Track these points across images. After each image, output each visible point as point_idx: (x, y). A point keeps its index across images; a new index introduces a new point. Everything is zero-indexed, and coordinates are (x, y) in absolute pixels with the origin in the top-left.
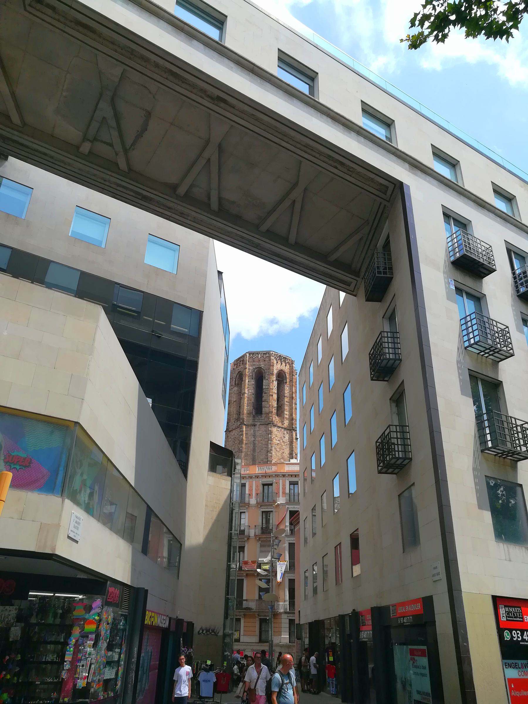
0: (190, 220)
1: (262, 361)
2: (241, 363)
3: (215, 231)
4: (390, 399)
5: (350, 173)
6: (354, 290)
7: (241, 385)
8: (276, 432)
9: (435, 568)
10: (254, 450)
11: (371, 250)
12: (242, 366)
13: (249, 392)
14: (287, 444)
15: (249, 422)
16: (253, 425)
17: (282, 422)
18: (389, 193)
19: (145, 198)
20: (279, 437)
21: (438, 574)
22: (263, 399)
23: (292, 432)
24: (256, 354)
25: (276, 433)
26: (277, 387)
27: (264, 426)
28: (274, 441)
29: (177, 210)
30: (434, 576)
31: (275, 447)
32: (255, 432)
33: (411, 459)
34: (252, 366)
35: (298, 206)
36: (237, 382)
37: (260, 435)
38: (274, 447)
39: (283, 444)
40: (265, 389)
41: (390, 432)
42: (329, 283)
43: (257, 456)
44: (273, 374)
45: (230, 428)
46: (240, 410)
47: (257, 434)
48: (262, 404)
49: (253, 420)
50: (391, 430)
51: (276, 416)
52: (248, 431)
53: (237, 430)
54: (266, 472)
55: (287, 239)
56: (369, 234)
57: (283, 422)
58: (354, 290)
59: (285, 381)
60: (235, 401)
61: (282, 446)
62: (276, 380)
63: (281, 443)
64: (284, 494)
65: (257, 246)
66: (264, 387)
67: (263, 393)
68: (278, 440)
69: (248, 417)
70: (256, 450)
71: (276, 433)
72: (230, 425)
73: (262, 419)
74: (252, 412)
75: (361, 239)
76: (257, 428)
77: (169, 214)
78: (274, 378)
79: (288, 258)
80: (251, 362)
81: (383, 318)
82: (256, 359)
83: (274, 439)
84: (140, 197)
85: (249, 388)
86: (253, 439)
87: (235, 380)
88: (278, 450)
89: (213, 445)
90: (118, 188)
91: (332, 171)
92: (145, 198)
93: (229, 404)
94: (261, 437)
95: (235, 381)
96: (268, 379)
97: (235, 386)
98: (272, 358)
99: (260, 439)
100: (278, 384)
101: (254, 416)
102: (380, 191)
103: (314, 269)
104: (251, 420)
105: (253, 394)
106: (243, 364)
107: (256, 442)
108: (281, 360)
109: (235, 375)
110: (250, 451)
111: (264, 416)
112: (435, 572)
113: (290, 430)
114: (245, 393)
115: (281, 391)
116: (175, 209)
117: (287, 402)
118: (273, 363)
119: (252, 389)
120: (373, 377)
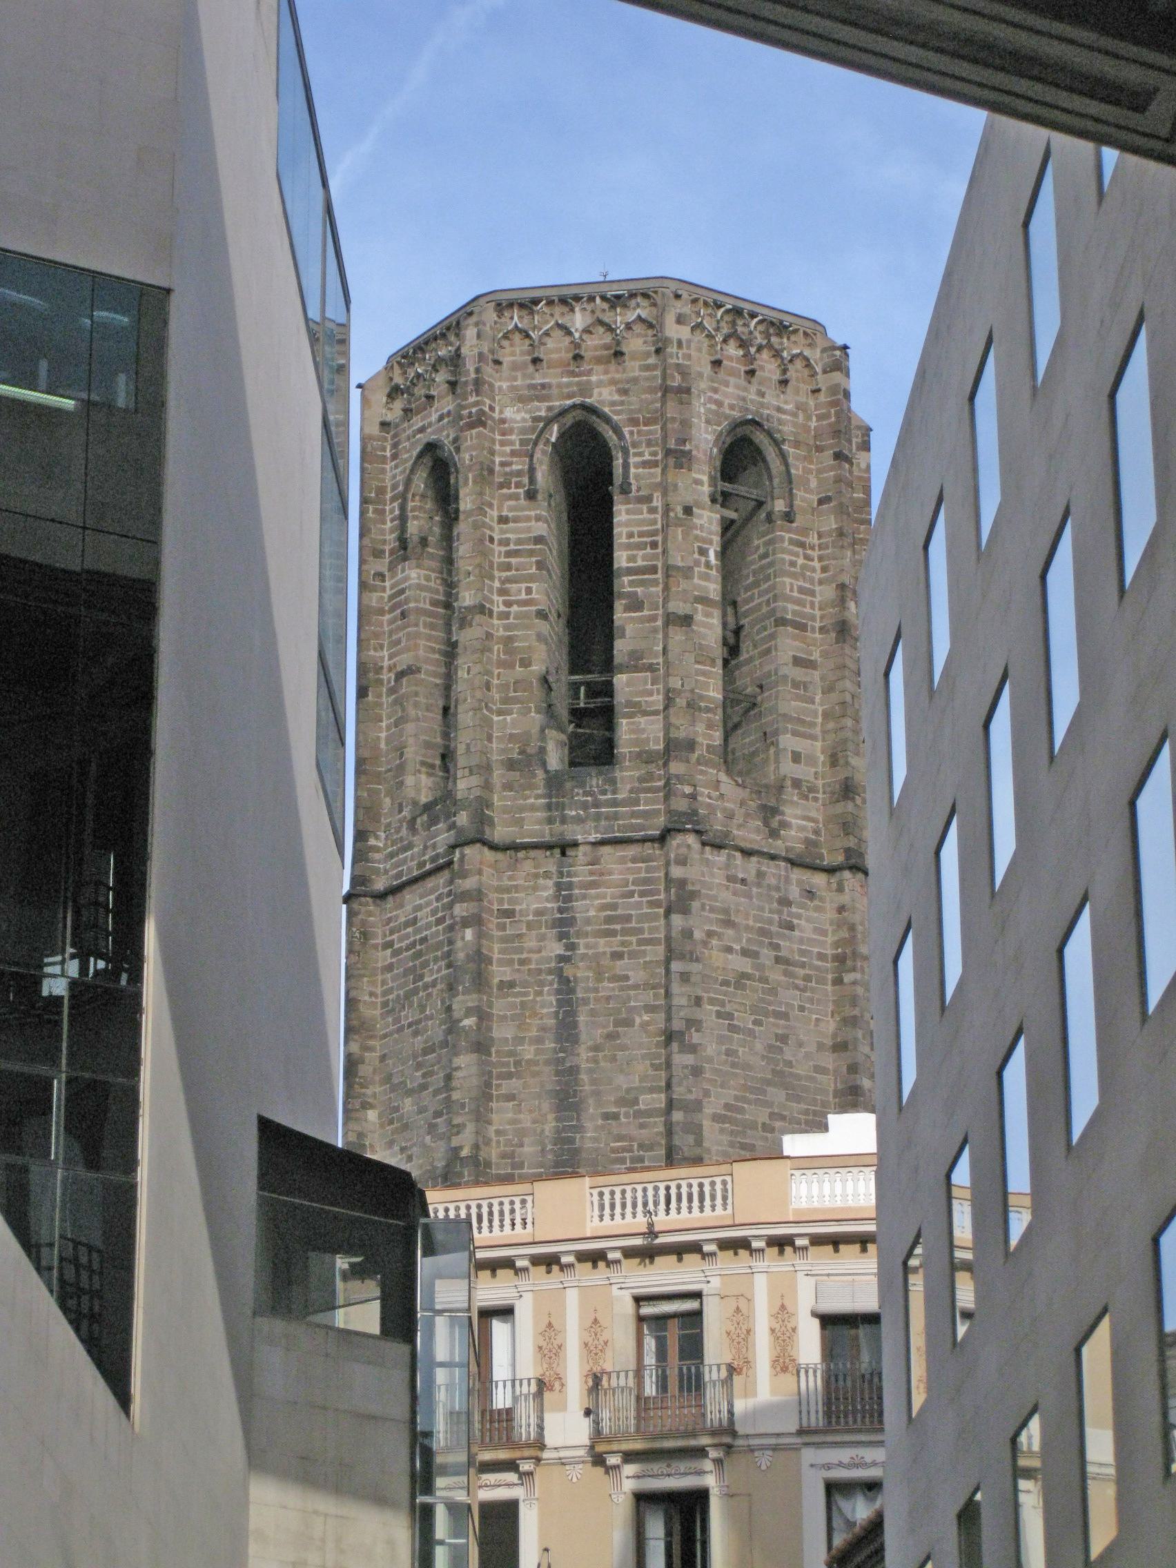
1: (599, 360)
2: (441, 377)
8: (725, 895)
10: (567, 1030)
13: (508, 604)
14: (807, 978)
15: (519, 822)
16: (549, 847)
17: (769, 812)
20: (747, 928)
22: (621, 647)
23: (840, 889)
25: (726, 897)
26: (723, 553)
27: (632, 851)
28: (716, 957)
31: (722, 1004)
32: (569, 899)
34: (521, 399)
37: (609, 920)
38: (712, 1001)
39: (776, 975)
40: (630, 571)
42: (1007, 99)
43: (590, 1071)
45: (377, 871)
47: (588, 909)
49: (549, 807)
51: (723, 777)
52: (516, 888)
53: (430, 883)
54: (651, 1225)
57: (774, 811)
59: (780, 506)
61: (773, 991)
63: (760, 967)
64: (784, 1369)
66: (621, 559)
67: (619, 605)
68: (745, 953)
69: (508, 787)
70: (582, 1026)
71: (726, 897)
72: (377, 850)
73: (614, 803)
74: (542, 750)
76: (580, 870)
80: (515, 367)
82: (550, 343)
83: (714, 942)
85: (508, 567)
87: (403, 508)
88: (745, 1020)
93: (362, 692)
94: (613, 933)
95: (403, 518)
96: (649, 499)
97: (405, 559)
98: (673, 331)
101: (554, 783)
104: (533, 808)
105: (542, 615)
106: (453, 385)
107: (581, 972)
108: (743, 344)
109: (393, 474)
110: (539, 1040)
111: (627, 774)
113: (831, 871)
114: (482, 609)
115: (747, 589)
117: (797, 661)
119: (531, 578)
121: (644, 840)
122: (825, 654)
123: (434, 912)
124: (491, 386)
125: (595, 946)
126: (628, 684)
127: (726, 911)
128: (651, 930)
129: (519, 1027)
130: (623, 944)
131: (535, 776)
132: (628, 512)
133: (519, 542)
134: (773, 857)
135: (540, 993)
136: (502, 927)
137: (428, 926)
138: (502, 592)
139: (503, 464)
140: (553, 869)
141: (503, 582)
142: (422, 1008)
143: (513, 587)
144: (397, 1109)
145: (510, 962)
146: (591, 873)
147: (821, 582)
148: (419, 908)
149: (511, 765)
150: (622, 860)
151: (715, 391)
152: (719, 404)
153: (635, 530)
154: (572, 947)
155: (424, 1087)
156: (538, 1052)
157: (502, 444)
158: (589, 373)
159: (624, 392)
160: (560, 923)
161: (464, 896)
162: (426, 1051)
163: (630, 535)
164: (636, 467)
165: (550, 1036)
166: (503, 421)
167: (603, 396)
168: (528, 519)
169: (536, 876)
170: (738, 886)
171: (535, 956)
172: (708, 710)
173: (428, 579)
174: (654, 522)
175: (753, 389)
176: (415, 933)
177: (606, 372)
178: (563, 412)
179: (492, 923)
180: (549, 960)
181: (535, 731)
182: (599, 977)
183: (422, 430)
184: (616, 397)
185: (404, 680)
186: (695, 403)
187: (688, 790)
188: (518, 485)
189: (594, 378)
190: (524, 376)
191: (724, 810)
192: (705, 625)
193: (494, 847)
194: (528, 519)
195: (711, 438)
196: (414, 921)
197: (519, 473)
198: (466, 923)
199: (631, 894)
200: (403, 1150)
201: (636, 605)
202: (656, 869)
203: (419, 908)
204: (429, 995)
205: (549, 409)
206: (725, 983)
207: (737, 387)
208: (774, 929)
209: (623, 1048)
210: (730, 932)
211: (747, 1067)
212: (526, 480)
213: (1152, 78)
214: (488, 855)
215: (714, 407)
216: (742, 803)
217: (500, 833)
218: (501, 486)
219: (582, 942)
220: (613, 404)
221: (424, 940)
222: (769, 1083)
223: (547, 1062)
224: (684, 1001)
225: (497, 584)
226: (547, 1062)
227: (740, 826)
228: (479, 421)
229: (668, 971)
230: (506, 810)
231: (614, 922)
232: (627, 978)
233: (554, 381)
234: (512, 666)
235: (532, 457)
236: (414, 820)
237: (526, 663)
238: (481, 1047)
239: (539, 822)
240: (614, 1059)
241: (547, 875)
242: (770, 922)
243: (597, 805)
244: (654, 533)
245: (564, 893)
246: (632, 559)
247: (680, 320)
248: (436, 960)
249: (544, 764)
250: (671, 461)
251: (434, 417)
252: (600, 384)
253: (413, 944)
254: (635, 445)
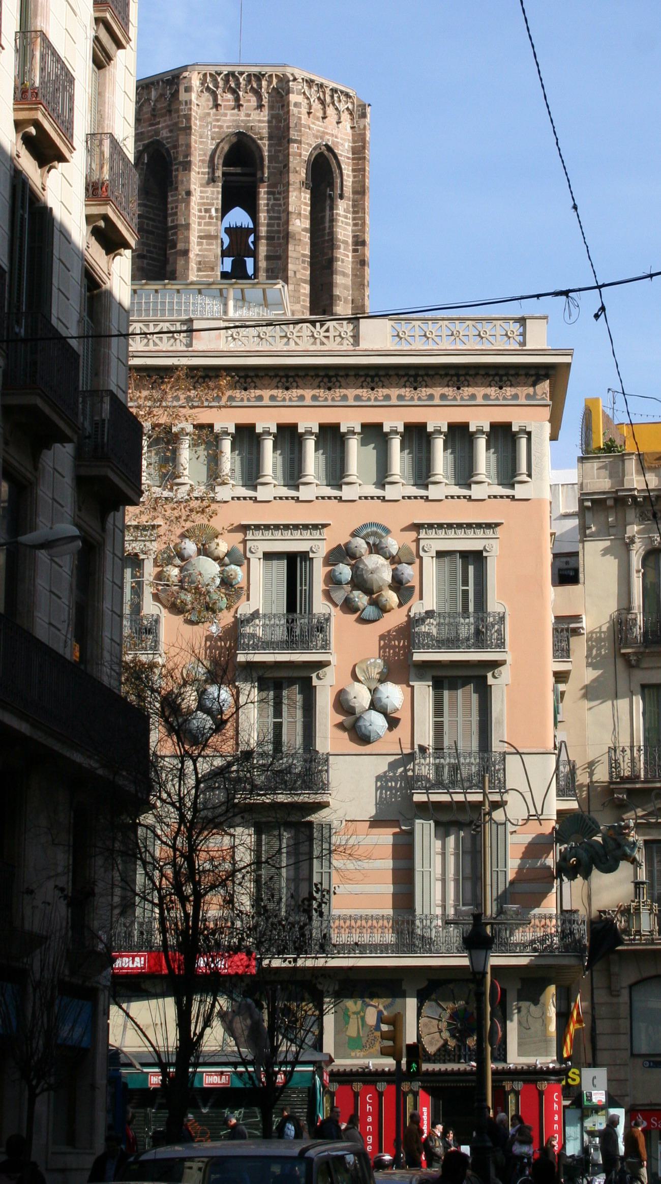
151: (218, 120)
158: (158, 123)
175: (242, 113)
189: (160, 126)
205: (144, 145)
207: (232, 115)
215: (217, 130)
220: (167, 138)
252: (163, 128)
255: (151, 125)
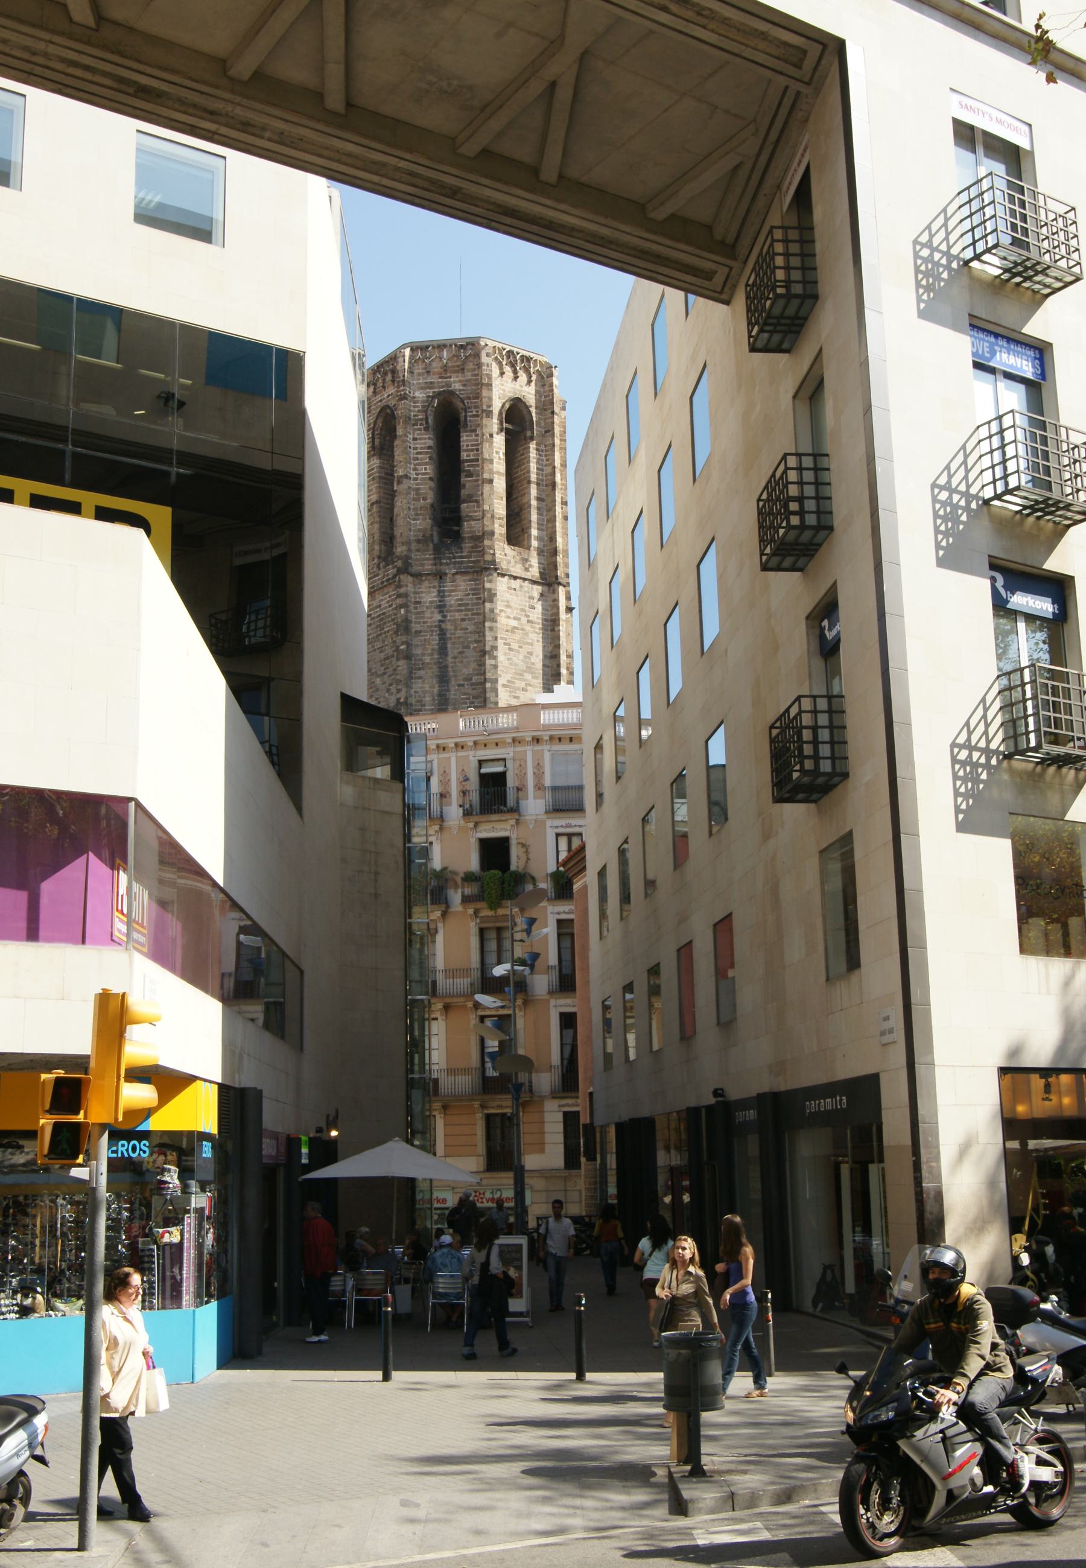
0: (270, 140)
1: (455, 372)
2: (389, 377)
3: (338, 161)
4: (807, 618)
5: (704, 21)
6: (723, 288)
7: (393, 451)
9: (887, 1019)
10: (443, 650)
11: (765, 195)
12: (391, 390)
15: (423, 565)
18: (809, 64)
19: (143, 92)
20: (516, 608)
21: (891, 1031)
22: (464, 493)
24: (434, 347)
27: (468, 577)
29: (232, 117)
30: (883, 1034)
31: (506, 639)
32: (443, 596)
33: (846, 775)
34: (422, 388)
35: (564, 94)
36: (377, 442)
37: (459, 605)
39: (528, 628)
41: (801, 712)
43: (452, 667)
44: (489, 414)
46: (392, 529)
47: (451, 601)
48: (457, 510)
49: (435, 559)
50: (803, 709)
51: (506, 546)
52: (422, 592)
53: (386, 590)
55: (536, 171)
56: (759, 155)
57: (527, 560)
58: (723, 288)
59: (529, 434)
60: (377, 502)
61: (526, 634)
62: (501, 430)
64: (539, 789)
65: (454, 193)
66: (464, 455)
67: (463, 475)
68: (515, 618)
69: (418, 550)
70: (449, 650)
73: (462, 557)
74: (432, 535)
75: (737, 168)
76: (448, 585)
77: (212, 127)
78: (493, 424)
79: (541, 218)
80: (419, 374)
81: (794, 397)
82: (434, 365)
83: (503, 614)
84: (131, 91)
85: (417, 459)
86: (438, 617)
88: (515, 646)
89: (349, 703)
90: (71, 70)
91: (656, 18)
92: (143, 92)
94: (461, 611)
96: (475, 431)
97: (374, 455)
98: (484, 359)
99: (458, 616)
100: (508, 443)
101: (437, 550)
102: (786, 61)
103: (611, 242)
104: (428, 559)
106: (393, 381)
107: (448, 626)
111: (467, 545)
112: (886, 1025)
114: (406, 477)
116: (227, 114)
118: (490, 377)
119: (426, 464)
120: (768, 561)
121: (474, 572)
122: (547, 495)
123: (388, 602)
124: (409, 383)
125: (454, 616)
126: (467, 507)
127: (508, 602)
128: (477, 609)
129: (423, 649)
130: (466, 615)
131: (428, 546)
132: (467, 436)
133: (421, 448)
134: (525, 579)
135: (432, 635)
136: (416, 608)
137: (385, 608)
138: (415, 469)
139: (414, 416)
140: (437, 584)
141: (415, 465)
142: (383, 641)
143: (419, 467)
144: (373, 683)
145: (419, 623)
146: (452, 586)
147: (546, 466)
148: (382, 600)
149: (419, 541)
150: (465, 581)
151: (502, 385)
152: (504, 390)
153: (470, 443)
154: (444, 616)
155: (384, 674)
156: (431, 659)
157: (414, 407)
158: (450, 377)
159: (464, 385)
160: (439, 607)
161: (399, 596)
162: (385, 659)
163: (467, 446)
164: (470, 416)
165: (436, 652)
166: (414, 397)
167: (457, 386)
168: (425, 439)
169: (430, 587)
170: (513, 591)
171: (429, 620)
172: (500, 519)
173: (383, 464)
174: (477, 440)
176: (380, 610)
177: (457, 377)
178: (439, 393)
179: (412, 606)
180: (435, 622)
181: (429, 527)
182: (456, 629)
183: (381, 401)
184: (461, 388)
185: (375, 506)
186: (494, 390)
187: (492, 552)
188: (421, 425)
190: (424, 379)
191: (506, 560)
192: (499, 483)
193: (412, 575)
194: (425, 439)
195: (500, 405)
196: (380, 606)
197: (421, 420)
198: (401, 606)
199: (469, 595)
200: (376, 699)
201: (470, 475)
202: (478, 584)
203: (382, 600)
204: (386, 637)
205: (434, 392)
206: (507, 631)
208: (527, 609)
209: (466, 657)
210: (509, 610)
211: (517, 665)
212: (424, 422)
213: (713, 266)
214: (410, 579)
216: (514, 557)
217: (416, 569)
218: (414, 425)
219: (449, 614)
220: (460, 390)
221: (384, 613)
222: (525, 671)
223: (435, 663)
224: (490, 638)
225: (412, 466)
226: (435, 663)
227: (513, 567)
228: (404, 397)
229: (484, 626)
230: (417, 560)
231: (462, 606)
232: (467, 629)
233: (436, 381)
234: (418, 500)
235: (426, 411)
236: (379, 564)
237: (425, 499)
238: (408, 657)
239: (431, 565)
240: (462, 662)
241: (434, 587)
242: (525, 606)
243: (454, 558)
244: (478, 445)
245: (441, 594)
246: (468, 456)
247: (488, 355)
248: (389, 622)
249: (432, 541)
250: (484, 415)
251: (386, 396)
252: (455, 382)
253: (380, 615)
254: (470, 408)
255: (441, 378)
